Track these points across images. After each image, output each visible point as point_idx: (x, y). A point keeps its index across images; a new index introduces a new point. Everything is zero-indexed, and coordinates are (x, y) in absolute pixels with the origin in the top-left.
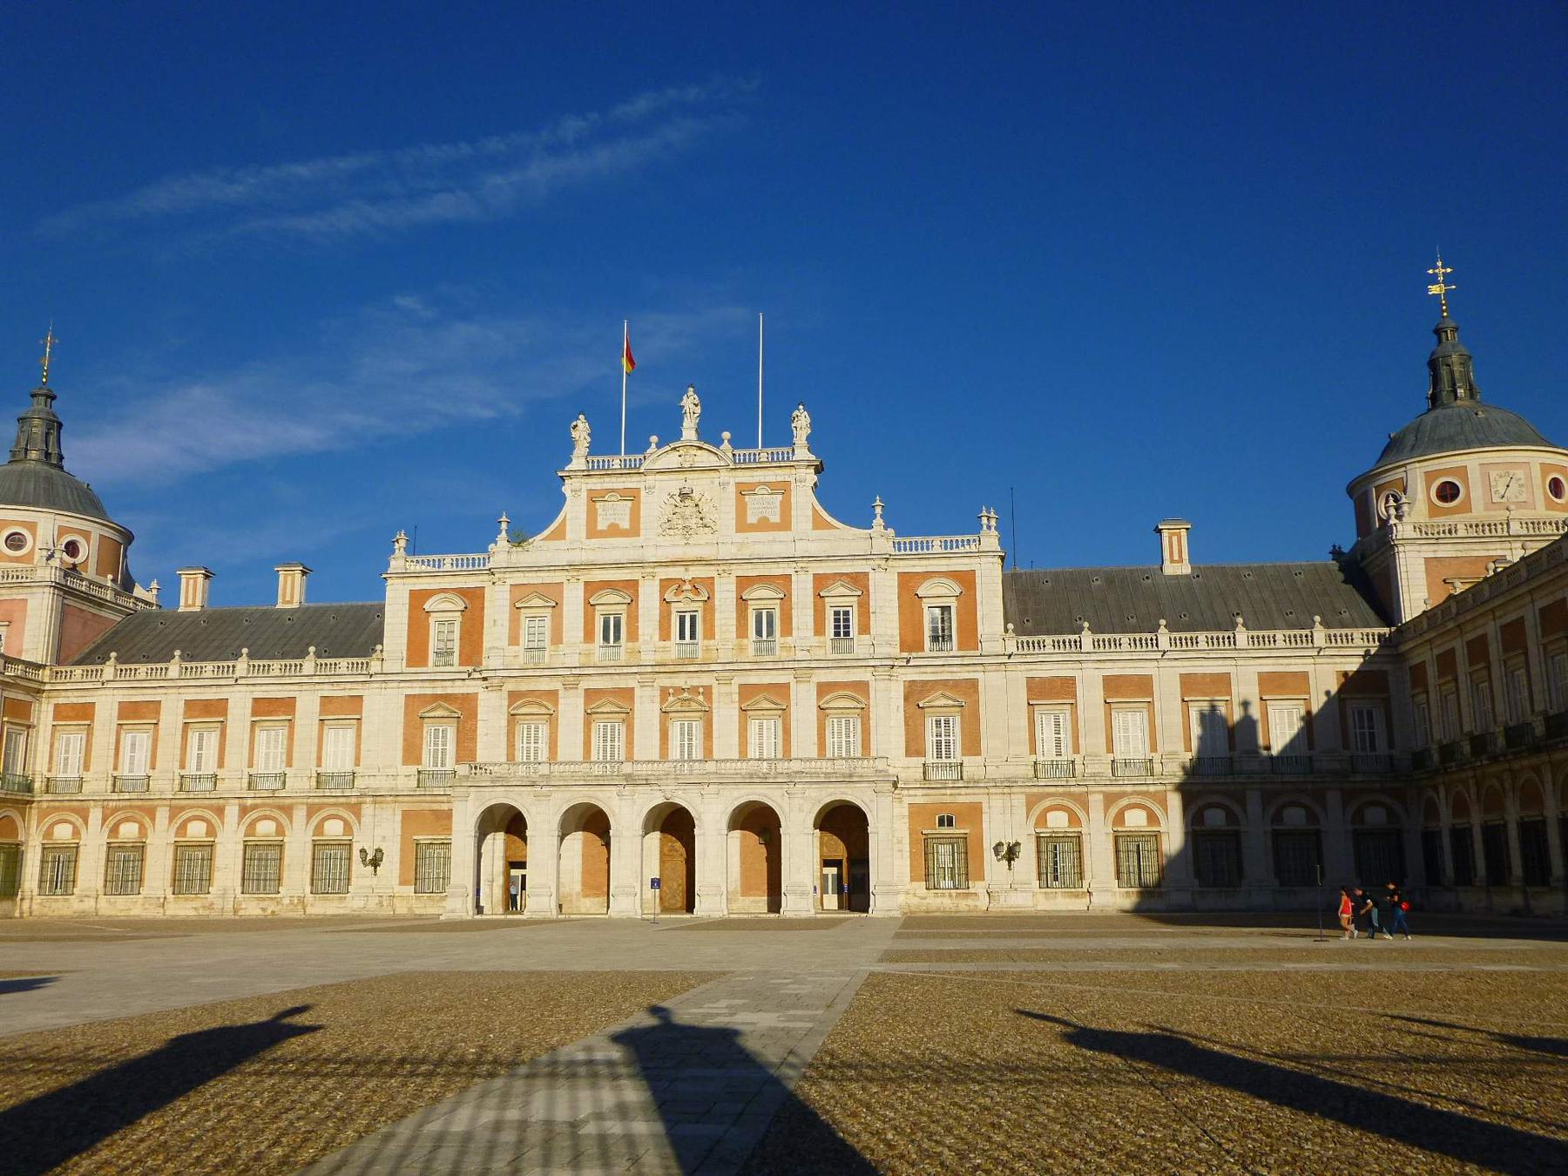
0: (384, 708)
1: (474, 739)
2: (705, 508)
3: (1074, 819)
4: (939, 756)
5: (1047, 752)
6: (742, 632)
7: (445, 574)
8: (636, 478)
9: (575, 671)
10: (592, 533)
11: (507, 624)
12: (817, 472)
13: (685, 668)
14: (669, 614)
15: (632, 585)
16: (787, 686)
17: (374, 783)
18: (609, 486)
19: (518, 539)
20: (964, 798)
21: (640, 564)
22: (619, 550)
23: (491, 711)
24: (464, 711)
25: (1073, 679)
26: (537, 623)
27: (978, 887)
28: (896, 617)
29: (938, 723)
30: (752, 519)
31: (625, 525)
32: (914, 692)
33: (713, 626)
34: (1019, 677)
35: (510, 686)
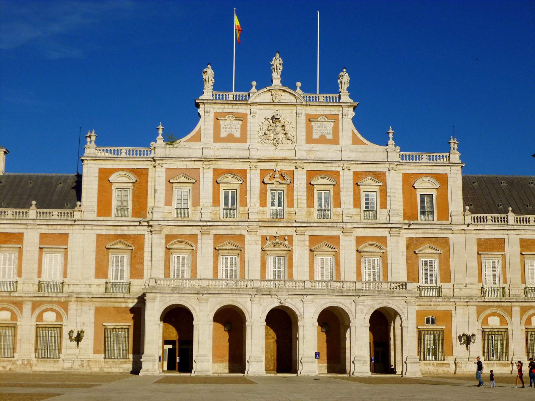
0: (83, 242)
1: (142, 263)
2: (287, 128)
3: (503, 321)
4: (426, 282)
5: (488, 282)
7: (123, 160)
8: (244, 107)
9: (209, 224)
10: (217, 138)
12: (355, 108)
13: (277, 224)
15: (242, 174)
16: (338, 237)
17: (77, 289)
18: (228, 111)
19: (170, 140)
20: (442, 307)
21: (248, 159)
23: (154, 247)
24: (135, 246)
25: (503, 240)
26: (181, 194)
27: (450, 360)
28: (402, 200)
29: (426, 263)
30: (315, 136)
31: (238, 135)
32: (412, 245)
34: (472, 237)
35: (167, 231)
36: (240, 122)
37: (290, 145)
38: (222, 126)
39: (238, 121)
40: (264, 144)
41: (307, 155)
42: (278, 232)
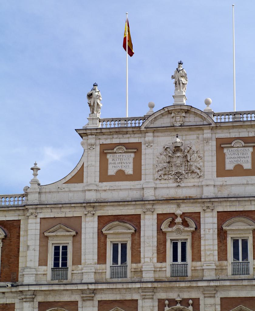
6: (222, 254)
11: (38, 248)
14: (165, 242)
21: (142, 201)
22: (124, 190)
30: (229, 166)
31: (129, 171)
33: (199, 251)
35: (40, 298)
36: (133, 155)
37: (196, 180)
38: (110, 161)
39: (129, 154)
40: (163, 181)
41: (219, 191)
42: (181, 295)
